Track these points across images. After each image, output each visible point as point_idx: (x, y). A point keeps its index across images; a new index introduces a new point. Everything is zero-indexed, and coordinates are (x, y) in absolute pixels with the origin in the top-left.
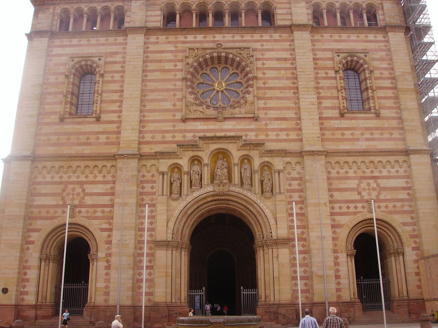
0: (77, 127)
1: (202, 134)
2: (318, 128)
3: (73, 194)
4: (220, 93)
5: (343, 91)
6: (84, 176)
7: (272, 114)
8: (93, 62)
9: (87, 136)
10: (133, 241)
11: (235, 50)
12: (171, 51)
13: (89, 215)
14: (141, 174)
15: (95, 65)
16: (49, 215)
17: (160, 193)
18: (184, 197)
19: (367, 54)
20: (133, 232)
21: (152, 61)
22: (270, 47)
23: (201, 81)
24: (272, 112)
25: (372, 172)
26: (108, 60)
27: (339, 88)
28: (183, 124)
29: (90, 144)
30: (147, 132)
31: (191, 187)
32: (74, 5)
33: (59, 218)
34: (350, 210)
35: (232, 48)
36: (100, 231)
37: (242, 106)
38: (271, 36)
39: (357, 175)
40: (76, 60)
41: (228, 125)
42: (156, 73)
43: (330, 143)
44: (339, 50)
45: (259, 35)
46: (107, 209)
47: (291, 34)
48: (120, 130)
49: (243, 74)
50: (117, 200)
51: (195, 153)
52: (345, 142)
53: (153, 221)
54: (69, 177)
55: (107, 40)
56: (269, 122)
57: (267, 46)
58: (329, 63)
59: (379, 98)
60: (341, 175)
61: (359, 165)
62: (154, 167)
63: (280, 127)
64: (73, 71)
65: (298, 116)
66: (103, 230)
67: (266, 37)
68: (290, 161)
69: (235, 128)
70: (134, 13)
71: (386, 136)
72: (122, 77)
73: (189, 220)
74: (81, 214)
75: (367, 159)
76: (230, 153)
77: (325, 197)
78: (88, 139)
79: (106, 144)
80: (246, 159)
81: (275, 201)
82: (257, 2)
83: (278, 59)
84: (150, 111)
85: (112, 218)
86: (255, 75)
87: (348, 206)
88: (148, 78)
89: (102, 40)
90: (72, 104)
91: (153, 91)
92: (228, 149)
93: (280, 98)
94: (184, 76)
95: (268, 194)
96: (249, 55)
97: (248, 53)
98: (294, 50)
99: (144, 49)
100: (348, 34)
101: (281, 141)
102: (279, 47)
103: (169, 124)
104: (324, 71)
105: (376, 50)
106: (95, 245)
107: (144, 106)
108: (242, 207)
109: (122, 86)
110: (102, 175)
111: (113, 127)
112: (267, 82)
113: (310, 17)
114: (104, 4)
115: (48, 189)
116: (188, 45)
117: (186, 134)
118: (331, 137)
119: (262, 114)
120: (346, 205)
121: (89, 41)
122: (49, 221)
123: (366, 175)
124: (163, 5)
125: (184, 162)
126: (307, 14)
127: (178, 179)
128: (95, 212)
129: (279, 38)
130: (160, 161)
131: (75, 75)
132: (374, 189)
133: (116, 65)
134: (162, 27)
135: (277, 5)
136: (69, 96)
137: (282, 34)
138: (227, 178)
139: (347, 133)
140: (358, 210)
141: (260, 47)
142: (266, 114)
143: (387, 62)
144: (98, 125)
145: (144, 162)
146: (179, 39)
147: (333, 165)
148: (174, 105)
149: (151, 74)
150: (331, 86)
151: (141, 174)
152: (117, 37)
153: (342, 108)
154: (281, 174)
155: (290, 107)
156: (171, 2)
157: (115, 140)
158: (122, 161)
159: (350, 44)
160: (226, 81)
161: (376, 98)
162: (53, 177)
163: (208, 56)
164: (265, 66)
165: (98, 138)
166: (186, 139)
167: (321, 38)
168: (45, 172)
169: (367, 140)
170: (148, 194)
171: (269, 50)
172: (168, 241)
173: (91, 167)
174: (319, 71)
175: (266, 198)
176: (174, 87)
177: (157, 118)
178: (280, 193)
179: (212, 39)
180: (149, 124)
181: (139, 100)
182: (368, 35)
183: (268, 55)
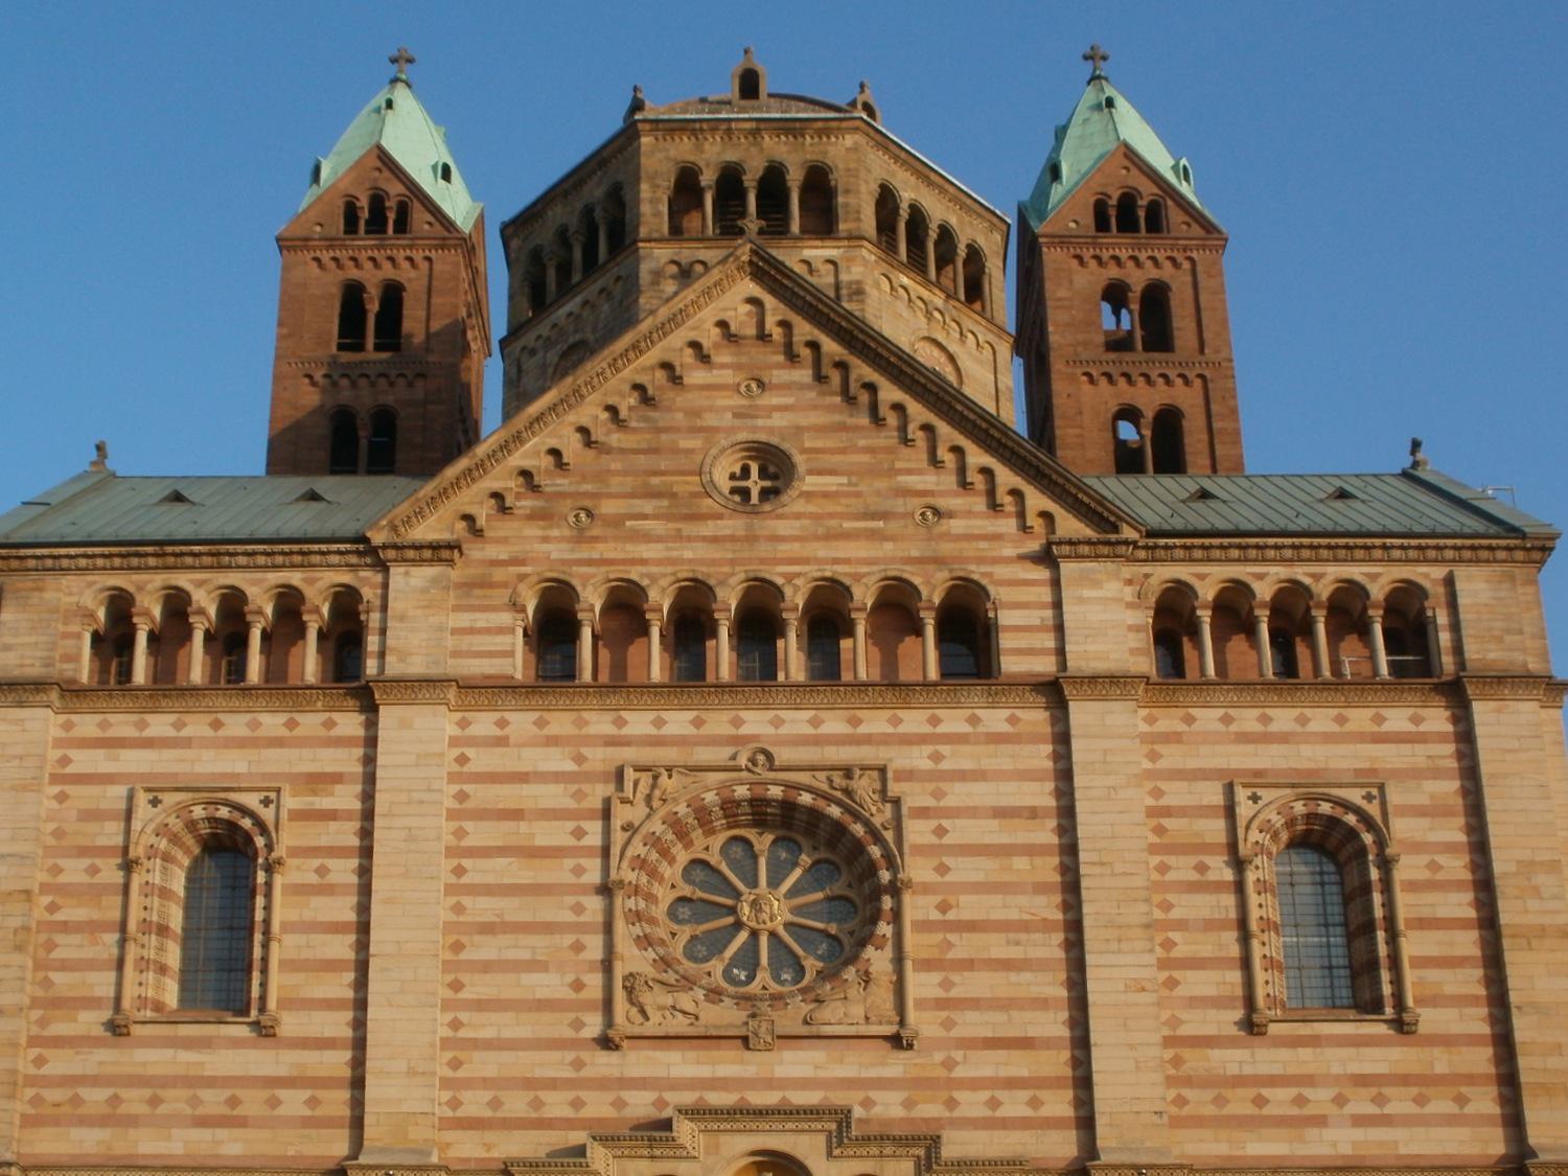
0: (185, 1056)
1: (688, 1098)
2: (1158, 1077)
7: (974, 1024)
9: (227, 1093)
11: (822, 776)
12: (557, 777)
21: (481, 815)
24: (971, 1016)
29: (241, 1122)
30: (468, 1084)
35: (813, 768)
38: (974, 720)
41: (795, 1063)
42: (500, 862)
43: (1207, 1133)
44: (1258, 773)
45: (923, 715)
55: (291, 724)
56: (958, 1055)
57: (957, 758)
67: (953, 721)
69: (821, 1074)
70: (402, 618)
78: (233, 1102)
79: (308, 1122)
82: (917, 581)
83: (1001, 813)
84: (480, 1005)
89: (272, 722)
91: (488, 929)
93: (1007, 965)
100: (1299, 711)
101: (1005, 1124)
102: (1007, 764)
103: (556, 1055)
104: (1193, 860)
112: (953, 902)
113: (1145, 640)
117: (627, 1095)
118: (1210, 1110)
121: (217, 725)
126: (1131, 628)
129: (1006, 728)
133: (333, 825)
137: (1018, 713)
141: (927, 764)
142: (948, 1024)
146: (592, 730)
148: (578, 986)
149: (482, 863)
150: (1217, 916)
155: (1046, 1000)
163: (710, 797)
164: (947, 840)
165: (274, 1103)
166: (628, 1113)
167: (1182, 727)
171: (962, 776)
177: (507, 1033)
179: (729, 730)
180: (477, 1056)
182: (1385, 712)
183: (959, 794)
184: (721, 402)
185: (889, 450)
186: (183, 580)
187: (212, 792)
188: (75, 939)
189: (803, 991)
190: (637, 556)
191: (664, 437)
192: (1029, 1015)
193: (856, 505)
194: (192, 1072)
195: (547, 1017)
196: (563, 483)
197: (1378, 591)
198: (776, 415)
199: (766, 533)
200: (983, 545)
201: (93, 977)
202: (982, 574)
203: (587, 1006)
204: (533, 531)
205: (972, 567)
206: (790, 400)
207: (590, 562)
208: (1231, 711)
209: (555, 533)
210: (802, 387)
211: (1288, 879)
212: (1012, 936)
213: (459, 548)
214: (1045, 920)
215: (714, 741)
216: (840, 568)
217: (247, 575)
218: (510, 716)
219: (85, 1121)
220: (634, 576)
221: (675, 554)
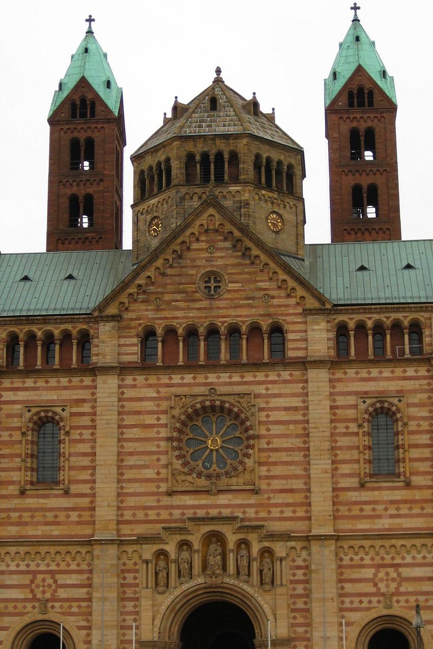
0: (41, 501)
2: (331, 503)
3: (44, 586)
4: (214, 453)
5: (367, 452)
6: (55, 563)
7: (277, 484)
8: (55, 413)
9: (54, 513)
10: (115, 642)
11: (232, 397)
13: (64, 610)
14: (122, 562)
15: (57, 418)
16: (17, 611)
17: (145, 585)
18: (171, 590)
19: (402, 399)
20: (115, 632)
21: (129, 413)
22: (277, 392)
23: (191, 436)
24: (276, 482)
25: (393, 558)
26: (74, 410)
27: (361, 449)
28: (169, 498)
30: (126, 508)
31: (179, 577)
32: (23, 327)
33: (29, 615)
34: (363, 605)
36: (77, 630)
37: (239, 475)
38: (279, 375)
39: (376, 562)
40: (34, 410)
41: (223, 499)
42: (135, 430)
43: (346, 521)
44: (366, 393)
45: (264, 374)
46: (84, 604)
47: (305, 372)
48: (93, 505)
49: (243, 428)
50: (96, 595)
51: (184, 537)
52: (364, 521)
53: (137, 617)
54: (38, 565)
55: (70, 381)
56: (272, 495)
57: (274, 389)
58: (351, 413)
59: (411, 460)
60: (354, 563)
61: (377, 550)
62: (135, 553)
63: (286, 501)
64: (31, 425)
65: (307, 487)
66: (80, 628)
67: (273, 376)
68: (295, 546)
70: (103, 342)
71: (416, 511)
72: (93, 434)
73: (177, 616)
74: (54, 610)
75: (388, 543)
76: (224, 535)
77: (331, 590)
79: (78, 523)
80: (244, 543)
81: (276, 595)
82: (262, 323)
83: (286, 409)
84: (130, 481)
85: (90, 614)
86: (256, 433)
87: (360, 600)
88: (125, 436)
89: (64, 381)
90: (32, 469)
91: (131, 454)
92: (222, 531)
93: (287, 463)
94: (169, 435)
95: (267, 587)
96: (249, 404)
97: (249, 400)
98: (307, 395)
99: (118, 395)
101: (286, 519)
102: (288, 391)
103: (152, 498)
104: (344, 425)
105: (415, 391)
106: (72, 645)
107: (122, 474)
108: (238, 600)
109: (93, 448)
110: (75, 563)
111: (85, 502)
113: (332, 344)
114: (63, 327)
115: (15, 580)
116: (173, 390)
117: (173, 511)
118: (347, 513)
119: (263, 486)
120: (359, 599)
121: (47, 382)
122: (18, 618)
123: (385, 562)
124: (140, 329)
125: (171, 548)
126: (328, 339)
127: (164, 568)
128: (71, 607)
129: (289, 378)
130: (144, 546)
131: (33, 430)
132: (393, 580)
133: (84, 418)
134: (139, 361)
135: (289, 326)
136: (29, 460)
137: (293, 372)
138: (221, 567)
139: (368, 508)
140: (372, 605)
141: (264, 392)
142: (269, 485)
143: (428, 408)
144: (67, 499)
145: (125, 548)
146: (162, 381)
147: (346, 551)
149: (129, 430)
151: (122, 562)
152: (83, 378)
153: (362, 475)
154: (284, 562)
156: (150, 324)
157: (89, 519)
158: (99, 546)
159: (381, 383)
160: (222, 437)
161: (407, 460)
162: (18, 565)
163: (198, 406)
165: (68, 516)
168: (8, 558)
169: (392, 516)
170: (130, 585)
172: (155, 642)
173: (63, 553)
174: (338, 425)
175: (265, 591)
176: (157, 450)
177: (138, 490)
178: (282, 585)
179: (204, 381)
180: (129, 499)
181: (115, 468)
182: (407, 369)
183: (275, 402)
184: (202, 256)
185: (255, 273)
186: (34, 328)
187: (46, 407)
188: (6, 460)
189: (227, 473)
190: (175, 316)
191: (184, 270)
192: (294, 481)
193: (243, 294)
194: (44, 506)
195: (149, 484)
196: (152, 288)
197: (406, 323)
198: (219, 260)
199: (215, 306)
200: (283, 309)
201: (12, 473)
202: (283, 320)
203: (162, 480)
204: (143, 307)
205: (280, 317)
206: (223, 254)
207: (160, 319)
208: (359, 370)
209: (150, 308)
210: (228, 249)
211: (376, 427)
212: (289, 453)
213: (121, 317)
214: (299, 447)
215: (199, 385)
216: (238, 319)
217: (54, 326)
218: (137, 377)
219: (12, 524)
220: (174, 324)
221: (187, 315)
